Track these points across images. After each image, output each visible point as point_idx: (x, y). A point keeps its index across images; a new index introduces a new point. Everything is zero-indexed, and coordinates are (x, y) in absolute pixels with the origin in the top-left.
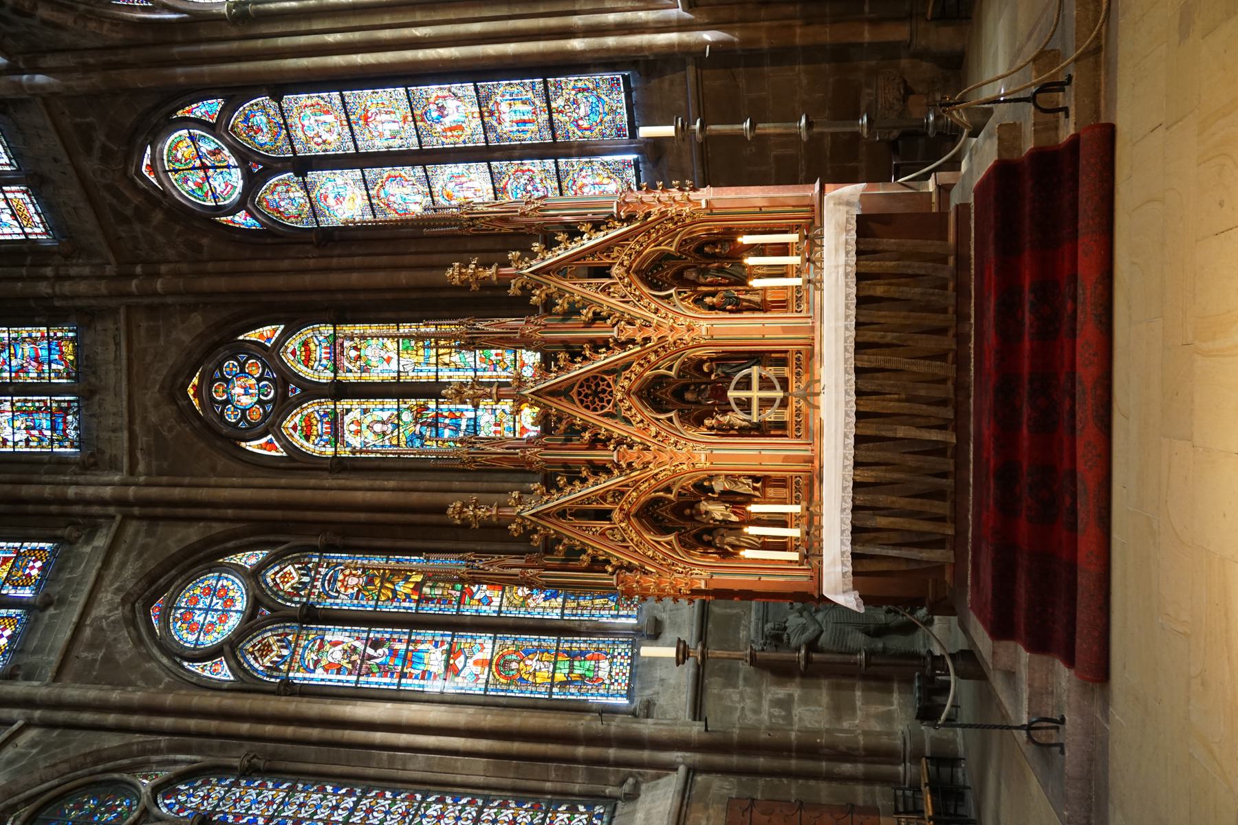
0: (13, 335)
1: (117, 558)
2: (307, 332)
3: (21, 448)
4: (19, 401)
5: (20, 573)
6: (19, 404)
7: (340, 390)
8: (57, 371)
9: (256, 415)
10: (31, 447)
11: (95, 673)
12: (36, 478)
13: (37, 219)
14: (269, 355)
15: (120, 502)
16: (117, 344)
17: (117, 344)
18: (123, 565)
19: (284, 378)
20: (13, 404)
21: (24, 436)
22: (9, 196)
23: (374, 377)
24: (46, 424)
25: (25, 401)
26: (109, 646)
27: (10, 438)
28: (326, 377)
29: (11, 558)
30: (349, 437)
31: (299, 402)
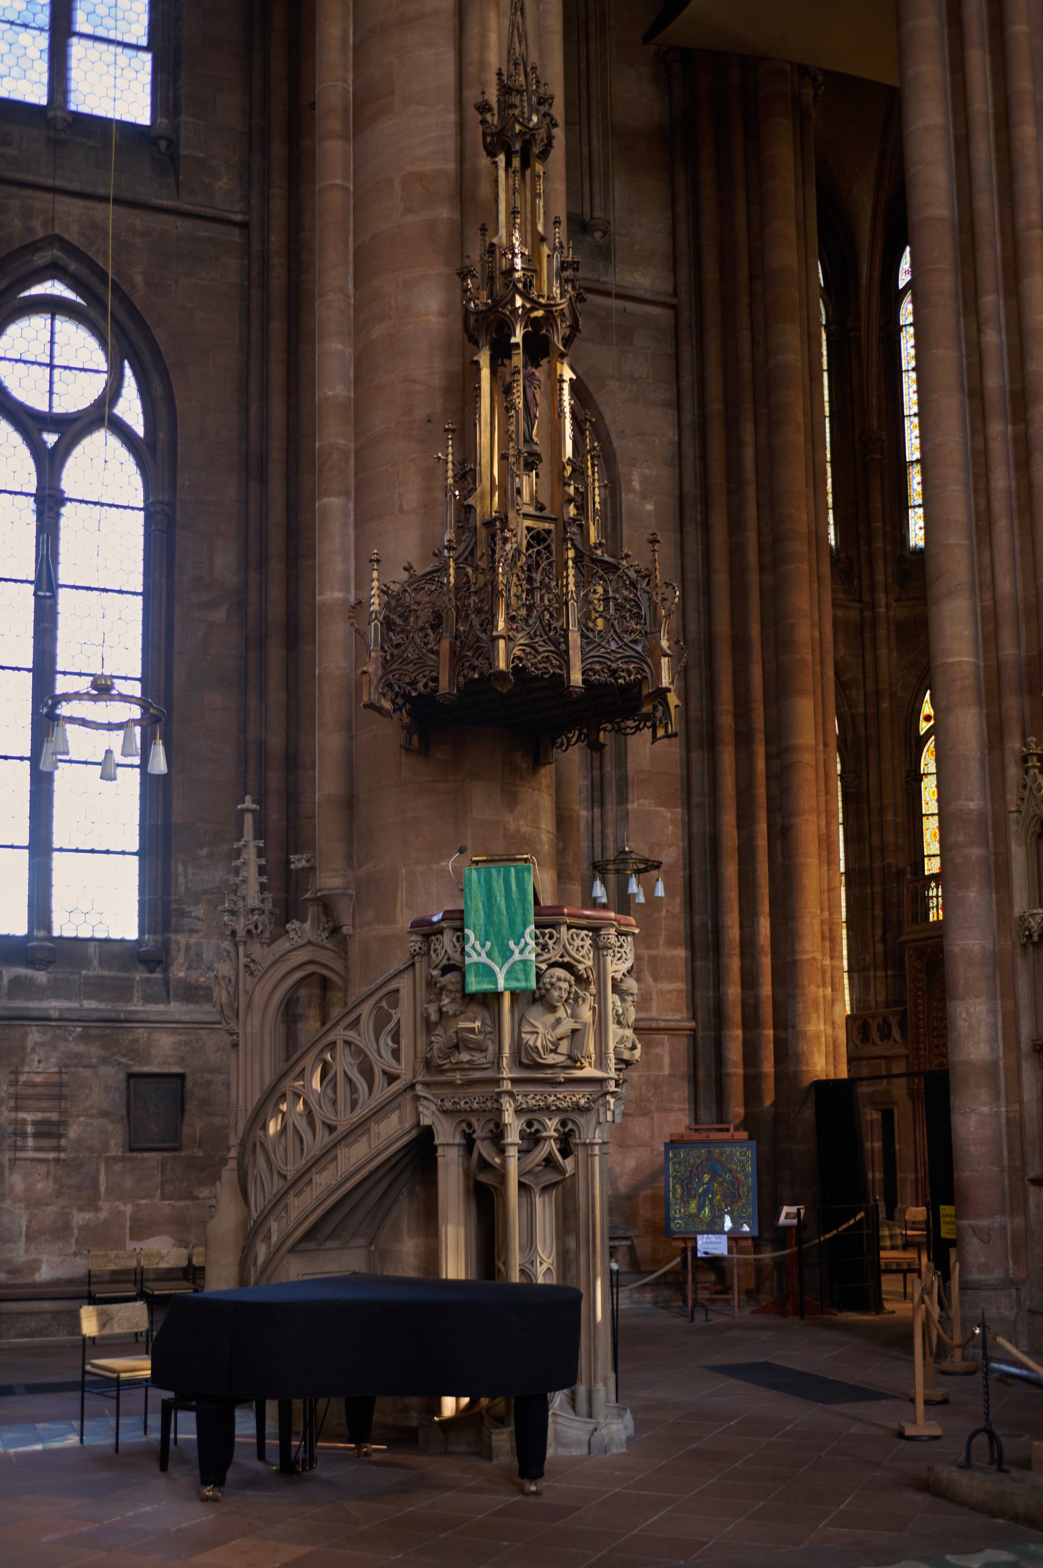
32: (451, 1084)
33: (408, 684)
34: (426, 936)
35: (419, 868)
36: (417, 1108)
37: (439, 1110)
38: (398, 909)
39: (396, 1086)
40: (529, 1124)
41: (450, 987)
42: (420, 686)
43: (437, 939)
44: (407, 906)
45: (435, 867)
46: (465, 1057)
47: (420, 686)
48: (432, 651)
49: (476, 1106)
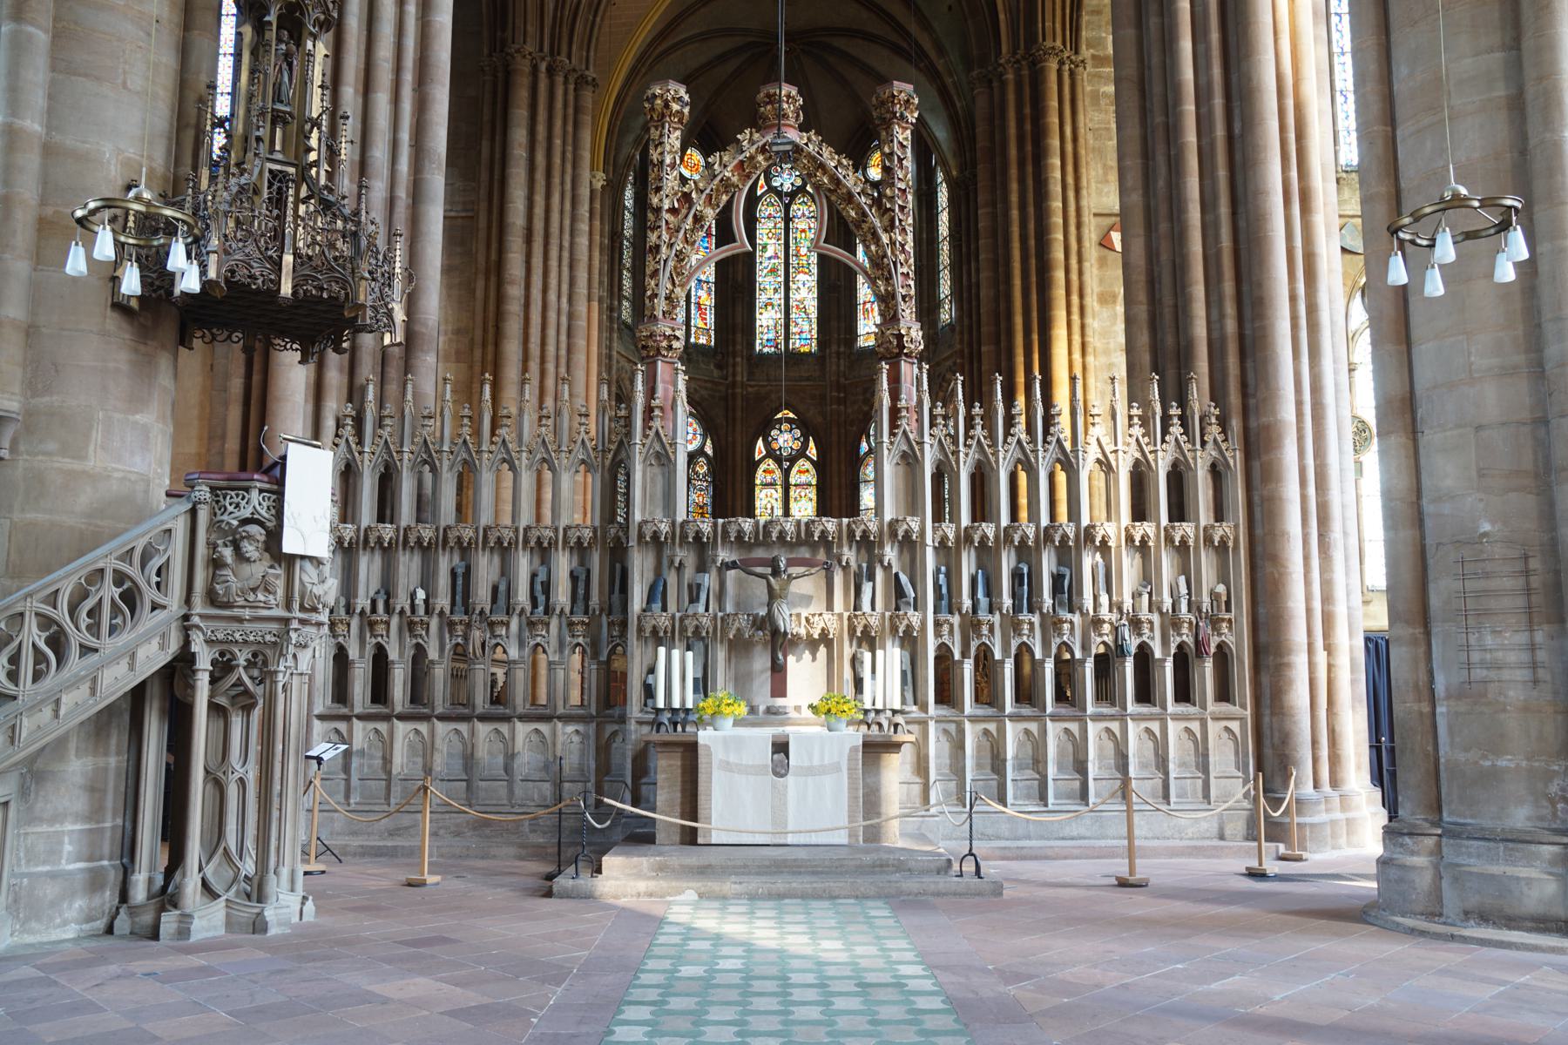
1: (709, 385)
2: (813, 471)
3: (758, 323)
7: (787, 487)
8: (796, 343)
9: (775, 446)
14: (802, 453)
15: (734, 384)
16: (808, 379)
17: (808, 379)
18: (706, 389)
19: (793, 460)
23: (792, 504)
24: (771, 336)
28: (792, 481)
30: (764, 491)
31: (780, 466)
32: (240, 620)
33: (249, 277)
34: (213, 489)
35: (117, 416)
36: (187, 636)
37: (206, 641)
38: (91, 448)
39: (160, 615)
40: (222, 654)
41: (259, 537)
42: (260, 281)
43: (237, 495)
44: (103, 448)
45: (130, 417)
46: (261, 597)
47: (260, 281)
48: (271, 257)
49: (252, 638)
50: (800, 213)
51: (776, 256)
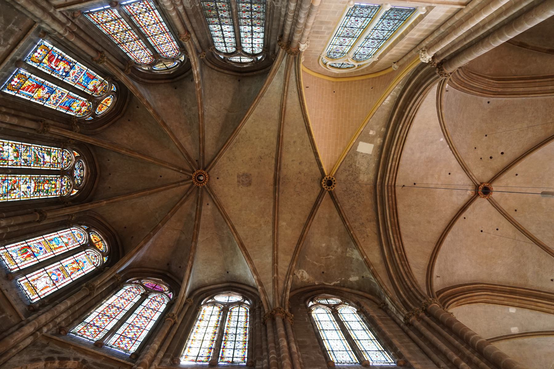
0: (6, 198)
4: (6, 165)
5: (21, 81)
6: (6, 164)
10: (2, 142)
11: (16, 17)
12: (8, 127)
13: (4, 257)
20: (8, 163)
21: (4, 147)
22: (16, 266)
25: (3, 165)
26: (4, 29)
27: (10, 147)
29: (21, 89)
50: (63, 183)
51: (45, 163)
